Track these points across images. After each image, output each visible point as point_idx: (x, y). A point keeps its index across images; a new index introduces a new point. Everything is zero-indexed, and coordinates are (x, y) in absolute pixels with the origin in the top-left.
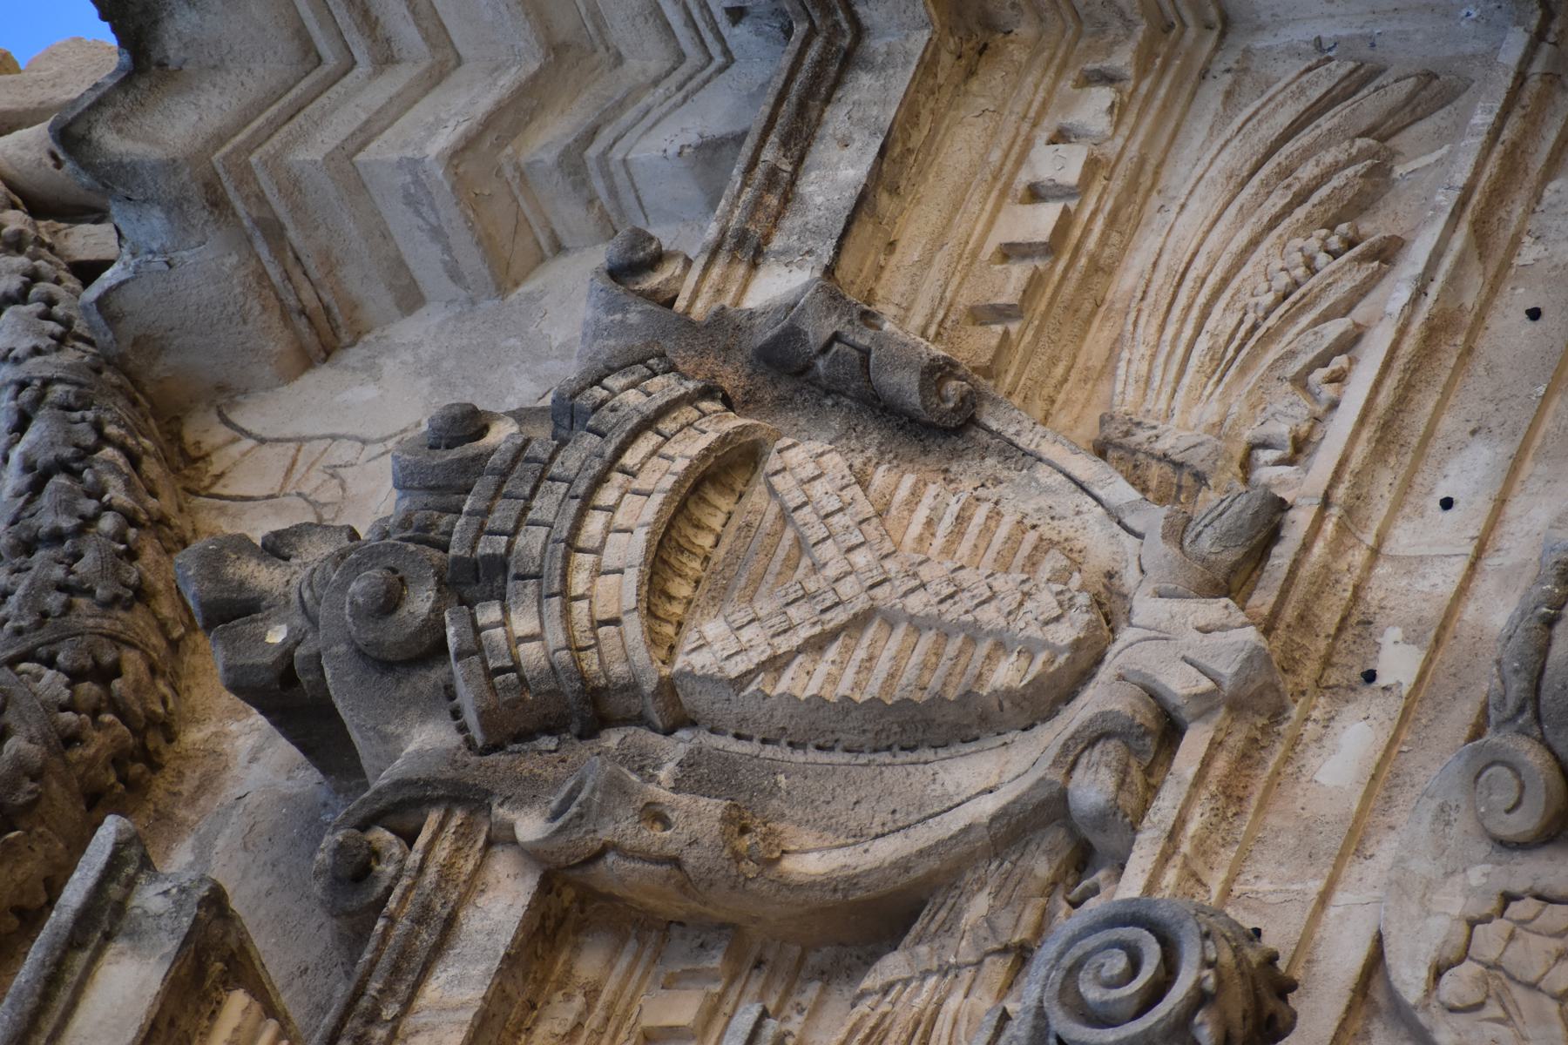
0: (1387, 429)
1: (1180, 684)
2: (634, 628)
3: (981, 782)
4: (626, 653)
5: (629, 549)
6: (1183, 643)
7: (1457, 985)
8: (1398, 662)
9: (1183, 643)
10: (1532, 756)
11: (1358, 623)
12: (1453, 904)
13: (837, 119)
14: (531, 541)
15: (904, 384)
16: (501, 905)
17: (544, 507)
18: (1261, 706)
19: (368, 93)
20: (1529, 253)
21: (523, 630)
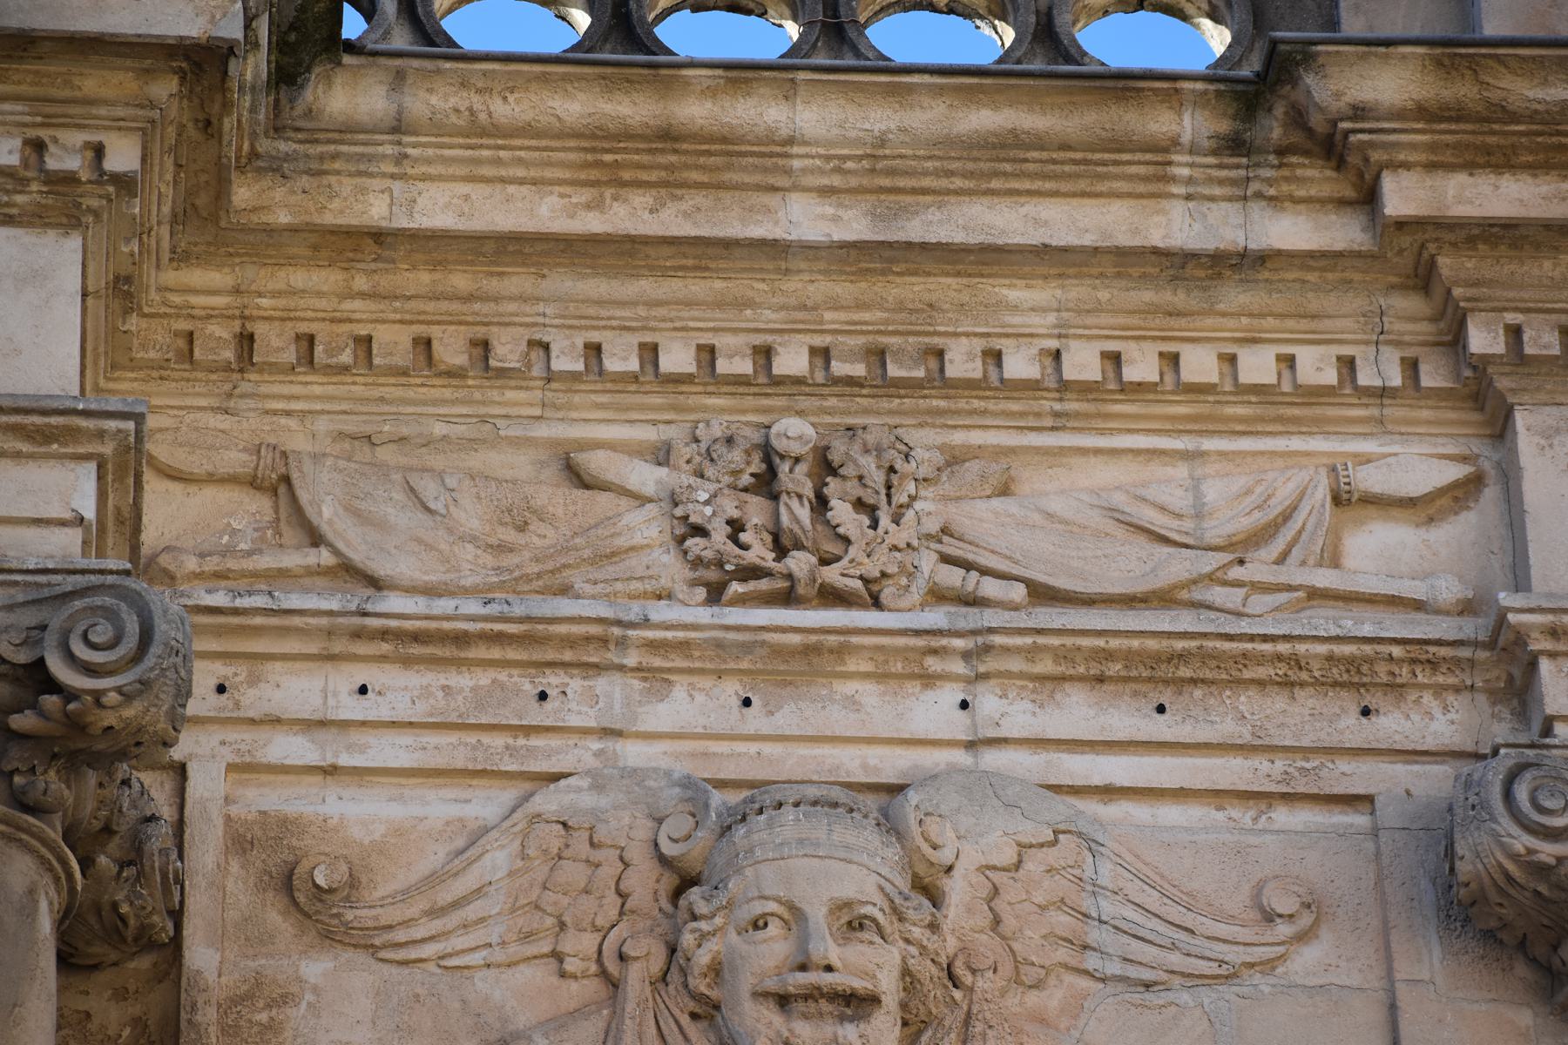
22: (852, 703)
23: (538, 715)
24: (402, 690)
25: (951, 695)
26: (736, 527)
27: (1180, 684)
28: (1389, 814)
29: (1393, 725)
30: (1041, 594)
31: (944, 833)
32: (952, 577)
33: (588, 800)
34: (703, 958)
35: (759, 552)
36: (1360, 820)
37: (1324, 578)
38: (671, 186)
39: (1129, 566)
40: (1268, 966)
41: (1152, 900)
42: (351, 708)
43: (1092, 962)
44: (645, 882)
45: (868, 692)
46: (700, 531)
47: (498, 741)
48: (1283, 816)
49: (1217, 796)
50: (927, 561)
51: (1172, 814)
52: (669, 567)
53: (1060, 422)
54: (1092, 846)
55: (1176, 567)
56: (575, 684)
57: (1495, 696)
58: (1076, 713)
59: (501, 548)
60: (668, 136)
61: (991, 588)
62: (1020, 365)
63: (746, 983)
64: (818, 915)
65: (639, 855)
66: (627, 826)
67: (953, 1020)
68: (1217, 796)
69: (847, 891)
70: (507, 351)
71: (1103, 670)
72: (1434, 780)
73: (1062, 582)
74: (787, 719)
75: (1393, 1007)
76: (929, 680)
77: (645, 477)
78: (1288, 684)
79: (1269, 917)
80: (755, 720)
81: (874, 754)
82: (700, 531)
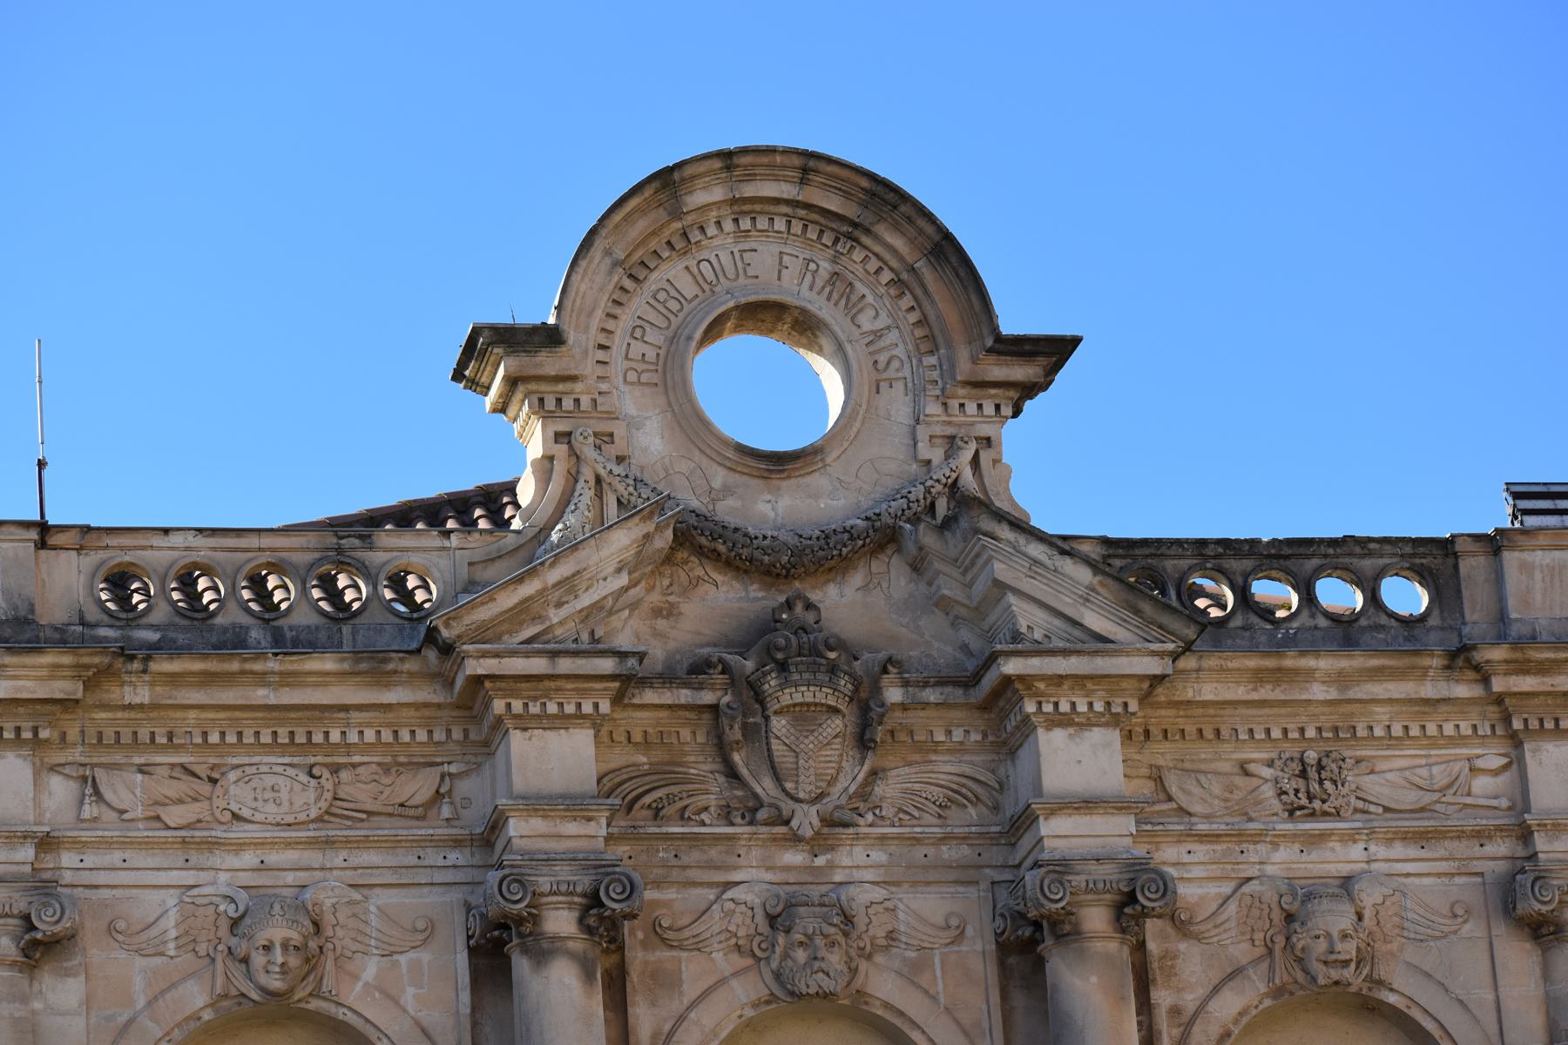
0: (883, 838)
1: (794, 824)
2: (777, 707)
3: (765, 787)
4: (773, 707)
5: (798, 698)
6: (807, 819)
7: (731, 905)
8: (820, 861)
9: (807, 819)
10: (779, 909)
11: (832, 848)
12: (749, 898)
13: (949, 689)
14: (796, 677)
15: (867, 736)
16: (708, 697)
17: (806, 676)
18: (796, 839)
19: (955, 573)
20: (944, 848)
21: (772, 682)
22: (1333, 850)
23: (1241, 858)
24: (1201, 851)
25: (1362, 845)
26: (1297, 791)
27: (1428, 839)
28: (1488, 878)
29: (1490, 849)
30: (1387, 809)
31: (1363, 896)
32: (1360, 804)
33: (1258, 888)
34: (1300, 946)
35: (1304, 801)
36: (1479, 880)
37: (1469, 800)
38: (1277, 683)
39: (1410, 798)
40: (1455, 932)
41: (1422, 911)
42: (1186, 858)
43: (1405, 933)
44: (1277, 916)
45: (1337, 846)
46: (1285, 793)
47: (1229, 867)
48: (1457, 880)
49: (1439, 875)
50: (1353, 800)
51: (1426, 881)
52: (1276, 805)
53: (1389, 747)
54: (1404, 895)
55: (1427, 798)
56: (1251, 847)
57: (1518, 838)
58: (1398, 850)
59: (1226, 800)
60: (1279, 670)
61: (1372, 808)
62: (1378, 732)
63: (1314, 956)
64: (1335, 935)
65: (1275, 906)
66: (1270, 897)
67: (1368, 958)
68: (1439, 875)
69: (1343, 927)
70: (1225, 733)
71: (1407, 837)
72: (1501, 867)
73: (1392, 806)
74: (1314, 856)
75: (1491, 943)
76: (1355, 841)
77: (1267, 772)
78: (1459, 837)
79: (1455, 916)
80: (1305, 857)
81: (1340, 866)
82: (1285, 793)
